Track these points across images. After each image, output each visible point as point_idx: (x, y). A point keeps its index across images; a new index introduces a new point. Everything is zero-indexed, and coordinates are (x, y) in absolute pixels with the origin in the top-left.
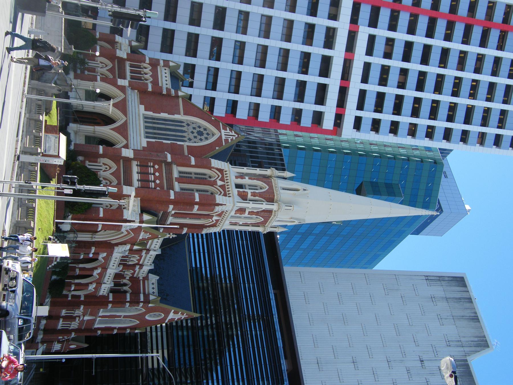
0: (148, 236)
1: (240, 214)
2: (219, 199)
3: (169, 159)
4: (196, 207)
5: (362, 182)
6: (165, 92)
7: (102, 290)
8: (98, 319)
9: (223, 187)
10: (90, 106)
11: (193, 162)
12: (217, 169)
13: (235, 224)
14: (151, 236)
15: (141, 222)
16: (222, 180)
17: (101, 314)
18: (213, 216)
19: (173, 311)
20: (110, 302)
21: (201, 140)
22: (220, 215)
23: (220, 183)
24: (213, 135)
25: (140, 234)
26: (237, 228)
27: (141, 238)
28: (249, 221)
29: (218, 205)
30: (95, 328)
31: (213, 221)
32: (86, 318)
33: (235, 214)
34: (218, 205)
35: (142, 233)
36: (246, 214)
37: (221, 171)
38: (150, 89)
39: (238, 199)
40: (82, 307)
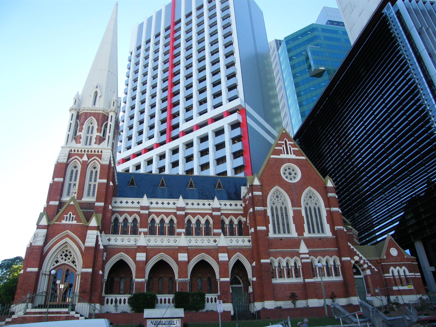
1: (81, 138)
5: (311, 76)
7: (240, 243)
8: (306, 234)
14: (71, 212)
17: (294, 234)
18: (83, 161)
19: (272, 156)
20: (255, 229)
25: (65, 224)
27: (75, 222)
28: (96, 127)
30: (333, 234)
31: (95, 159)
32: (303, 249)
33: (80, 143)
35: (64, 222)
40: (263, 261)
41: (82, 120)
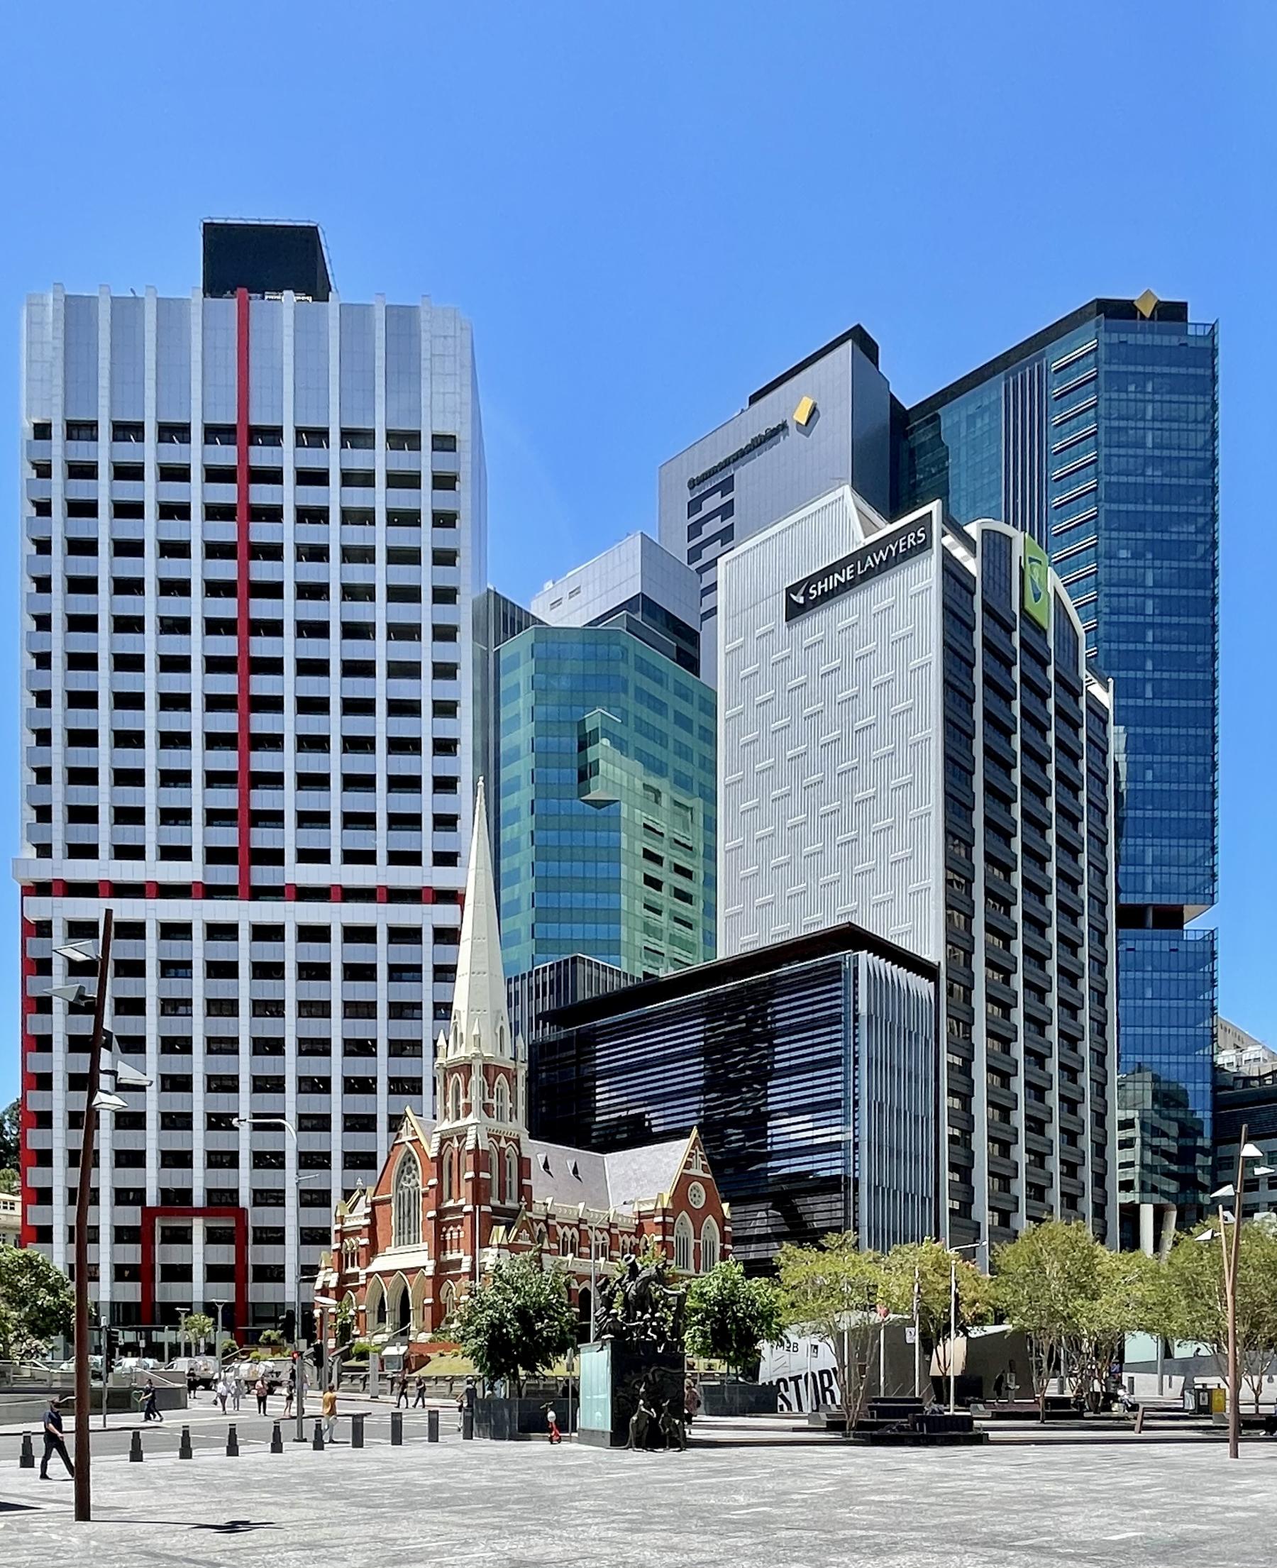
0: (524, 1233)
2: (470, 1145)
3: (432, 1214)
4: (482, 1175)
6: (368, 1221)
9: (460, 1139)
10: (392, 1317)
11: (434, 1181)
12: (441, 1148)
13: (513, 1112)
15: (499, 1246)
16: (451, 1139)
21: (416, 1169)
22: (498, 1139)
23: (456, 1145)
24: (409, 1152)
26: (522, 1108)
29: (477, 1145)
34: (477, 1145)
35: (520, 1242)
36: (494, 1101)
37: (442, 1142)
38: (365, 1241)
39: (471, 1119)
41: (491, 1079)
